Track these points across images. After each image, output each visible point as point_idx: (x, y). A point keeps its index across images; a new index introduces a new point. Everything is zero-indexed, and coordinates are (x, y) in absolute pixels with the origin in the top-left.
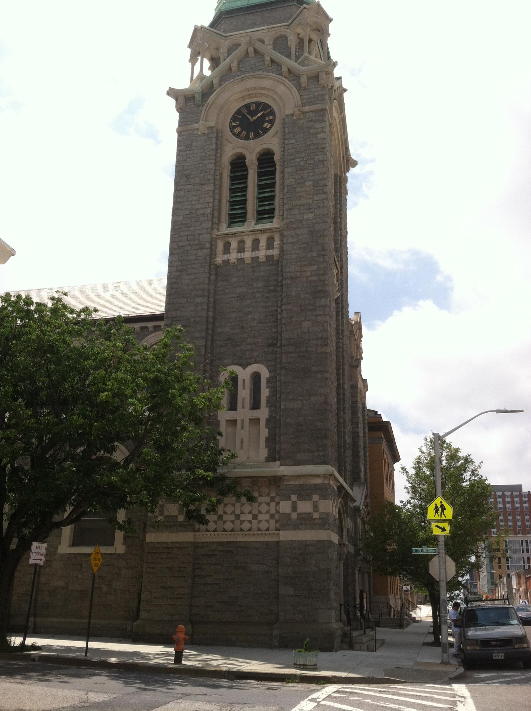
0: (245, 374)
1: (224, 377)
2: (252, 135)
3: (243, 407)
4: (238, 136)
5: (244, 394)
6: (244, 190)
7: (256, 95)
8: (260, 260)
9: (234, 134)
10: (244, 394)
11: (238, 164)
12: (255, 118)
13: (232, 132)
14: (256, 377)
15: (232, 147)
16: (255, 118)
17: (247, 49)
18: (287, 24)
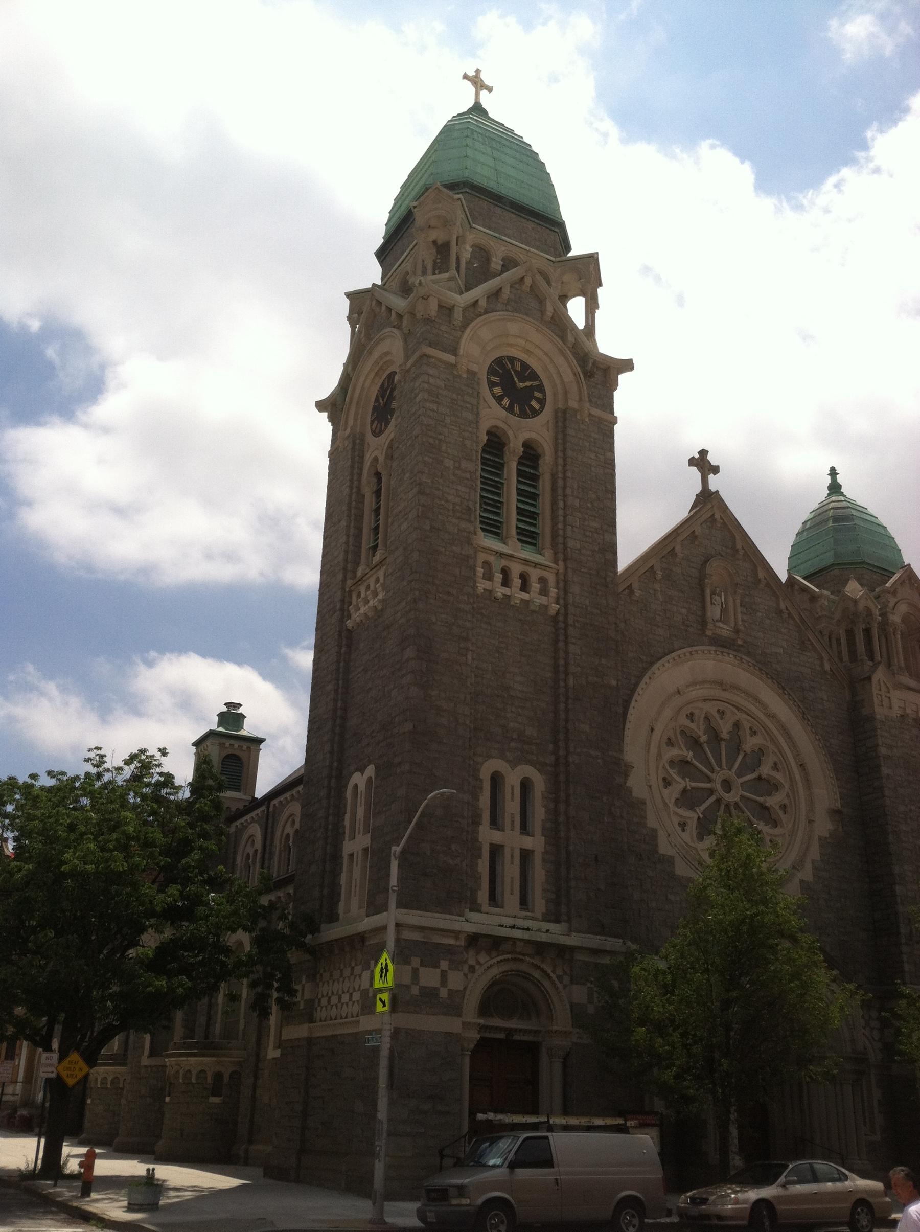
0: (513, 779)
1: (485, 773)
2: (517, 409)
3: (512, 830)
4: (499, 399)
5: (512, 806)
6: (498, 486)
7: (528, 352)
8: (532, 608)
9: (493, 395)
10: (512, 806)
11: (495, 444)
12: (522, 385)
13: (491, 391)
14: (526, 785)
15: (493, 413)
16: (522, 385)
17: (522, 279)
18: (553, 259)
